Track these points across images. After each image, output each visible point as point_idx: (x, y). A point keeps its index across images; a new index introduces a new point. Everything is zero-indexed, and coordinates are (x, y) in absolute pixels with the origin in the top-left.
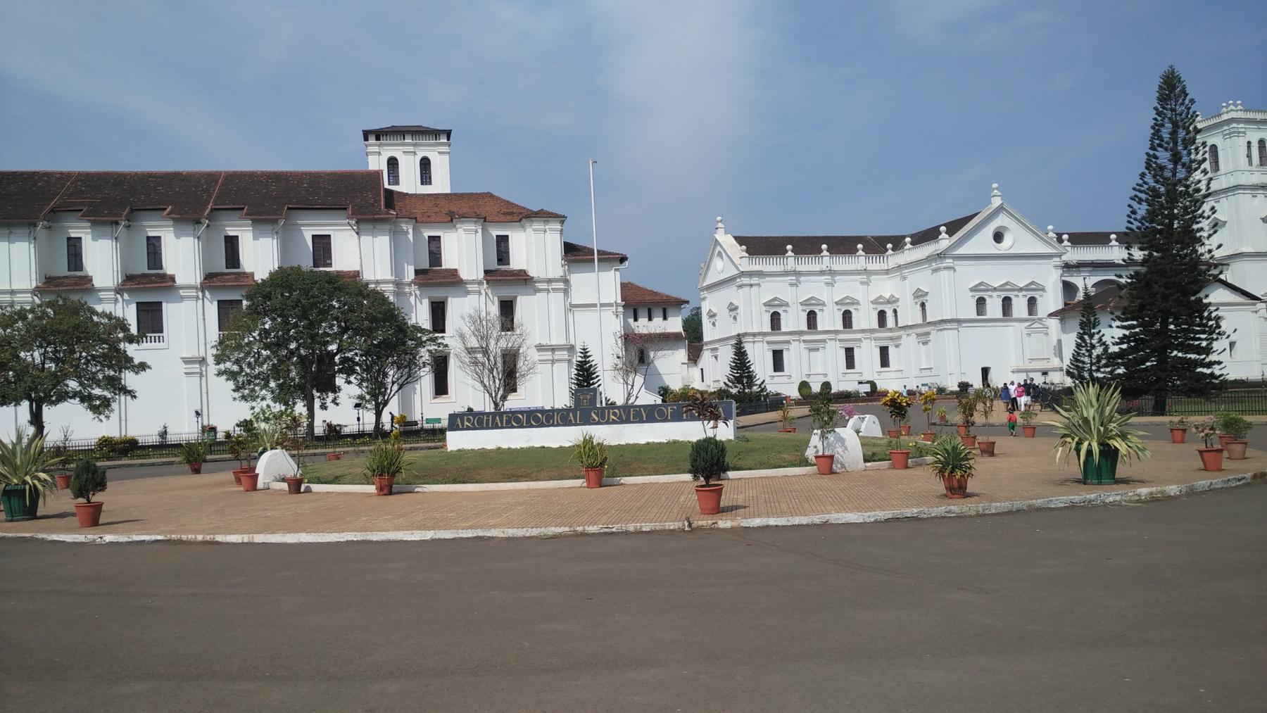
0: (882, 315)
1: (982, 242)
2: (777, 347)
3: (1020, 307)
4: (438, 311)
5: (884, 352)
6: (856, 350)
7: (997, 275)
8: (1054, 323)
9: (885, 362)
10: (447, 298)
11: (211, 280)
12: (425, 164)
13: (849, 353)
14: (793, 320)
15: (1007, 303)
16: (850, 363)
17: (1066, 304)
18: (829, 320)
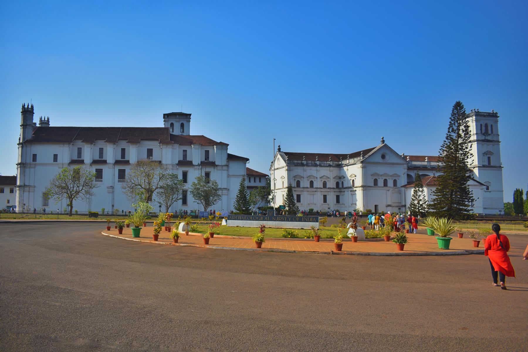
0: (337, 184)
2: (298, 193)
3: (390, 183)
5: (338, 198)
9: (338, 201)
13: (325, 197)
14: (305, 183)
16: (325, 200)
18: (318, 184)
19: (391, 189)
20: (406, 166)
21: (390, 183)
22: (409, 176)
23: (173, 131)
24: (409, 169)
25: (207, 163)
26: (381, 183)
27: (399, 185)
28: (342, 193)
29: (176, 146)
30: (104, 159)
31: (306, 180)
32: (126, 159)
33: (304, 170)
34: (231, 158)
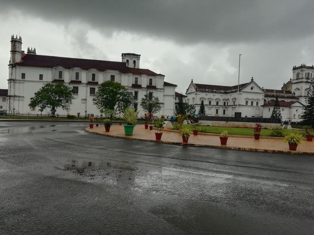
0: (225, 103)
1: (248, 89)
3: (255, 104)
4: (136, 93)
5: (224, 111)
6: (219, 110)
7: (251, 96)
8: (262, 107)
10: (138, 91)
11: (89, 83)
12: (134, 62)
13: (217, 110)
14: (206, 102)
15: (252, 102)
17: (264, 104)
19: (255, 107)
20: (264, 95)
21: (255, 104)
22: (265, 100)
23: (128, 65)
24: (266, 96)
25: (151, 87)
26: (249, 103)
27: (260, 104)
28: (227, 109)
29: (131, 75)
30: (79, 80)
31: (207, 100)
32: (96, 81)
33: (207, 95)
34: (166, 84)
